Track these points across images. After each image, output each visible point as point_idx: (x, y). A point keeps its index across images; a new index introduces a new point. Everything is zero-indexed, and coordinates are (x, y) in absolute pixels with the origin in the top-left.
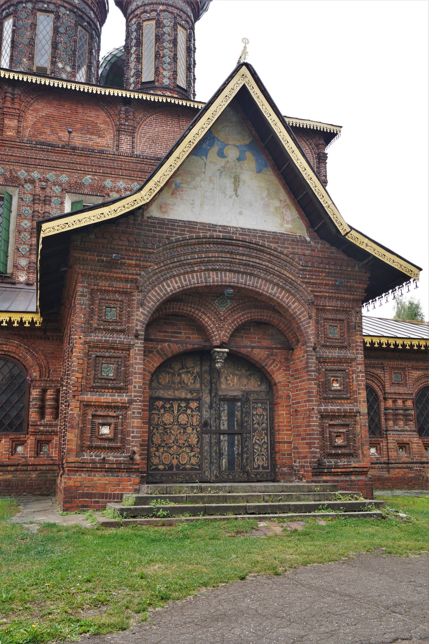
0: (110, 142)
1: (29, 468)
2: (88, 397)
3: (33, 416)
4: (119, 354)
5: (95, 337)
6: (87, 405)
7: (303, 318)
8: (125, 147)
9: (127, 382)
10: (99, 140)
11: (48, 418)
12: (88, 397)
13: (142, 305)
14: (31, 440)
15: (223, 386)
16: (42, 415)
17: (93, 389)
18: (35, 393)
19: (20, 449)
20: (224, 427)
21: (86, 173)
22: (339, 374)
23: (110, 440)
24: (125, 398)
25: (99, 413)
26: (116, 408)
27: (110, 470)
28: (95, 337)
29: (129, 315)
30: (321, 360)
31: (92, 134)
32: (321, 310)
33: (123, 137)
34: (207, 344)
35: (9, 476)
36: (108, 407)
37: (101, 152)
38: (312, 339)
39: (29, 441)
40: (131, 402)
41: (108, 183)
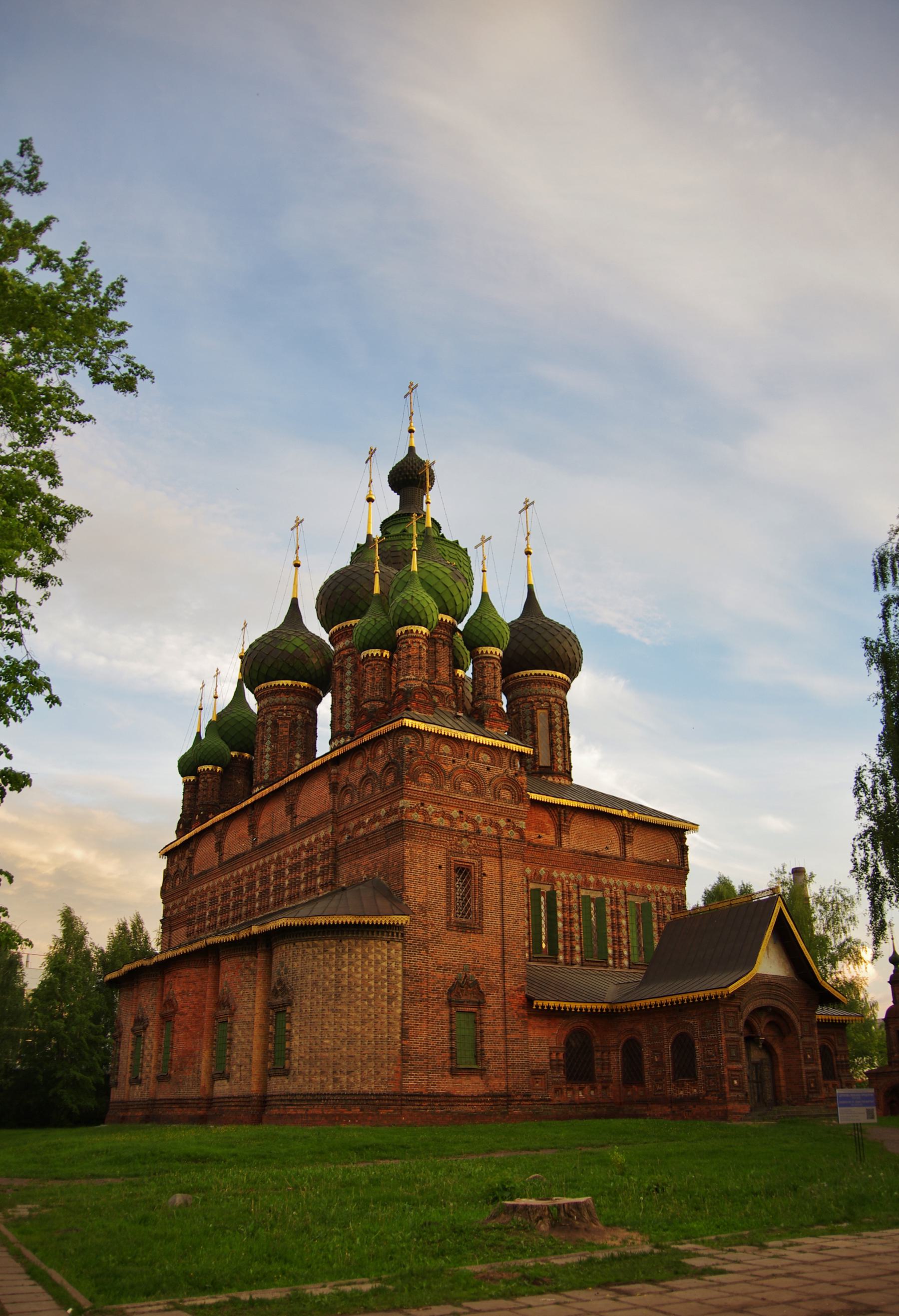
0: (554, 839)
1: (601, 1105)
2: (730, 1066)
3: (598, 1070)
4: (735, 1043)
5: (729, 1035)
6: (729, 1070)
7: (796, 1021)
8: (565, 844)
9: (741, 1058)
10: (546, 837)
11: (606, 1072)
12: (730, 1066)
13: (742, 1018)
14: (599, 1087)
15: (752, 1056)
16: (603, 1069)
17: (730, 1061)
18: (598, 1055)
19: (592, 1092)
20: (754, 1079)
21: (541, 866)
22: (810, 1050)
23: (737, 1086)
24: (740, 1066)
25: (733, 1073)
26: (738, 1071)
27: (740, 1102)
28: (729, 1035)
29: (738, 1024)
30: (804, 1043)
31: (542, 832)
32: (801, 1017)
33: (563, 835)
34: (754, 1035)
35: (594, 1110)
36: (735, 1070)
37: (552, 848)
38: (800, 1032)
39: (599, 1088)
40: (743, 1068)
41: (555, 874)
